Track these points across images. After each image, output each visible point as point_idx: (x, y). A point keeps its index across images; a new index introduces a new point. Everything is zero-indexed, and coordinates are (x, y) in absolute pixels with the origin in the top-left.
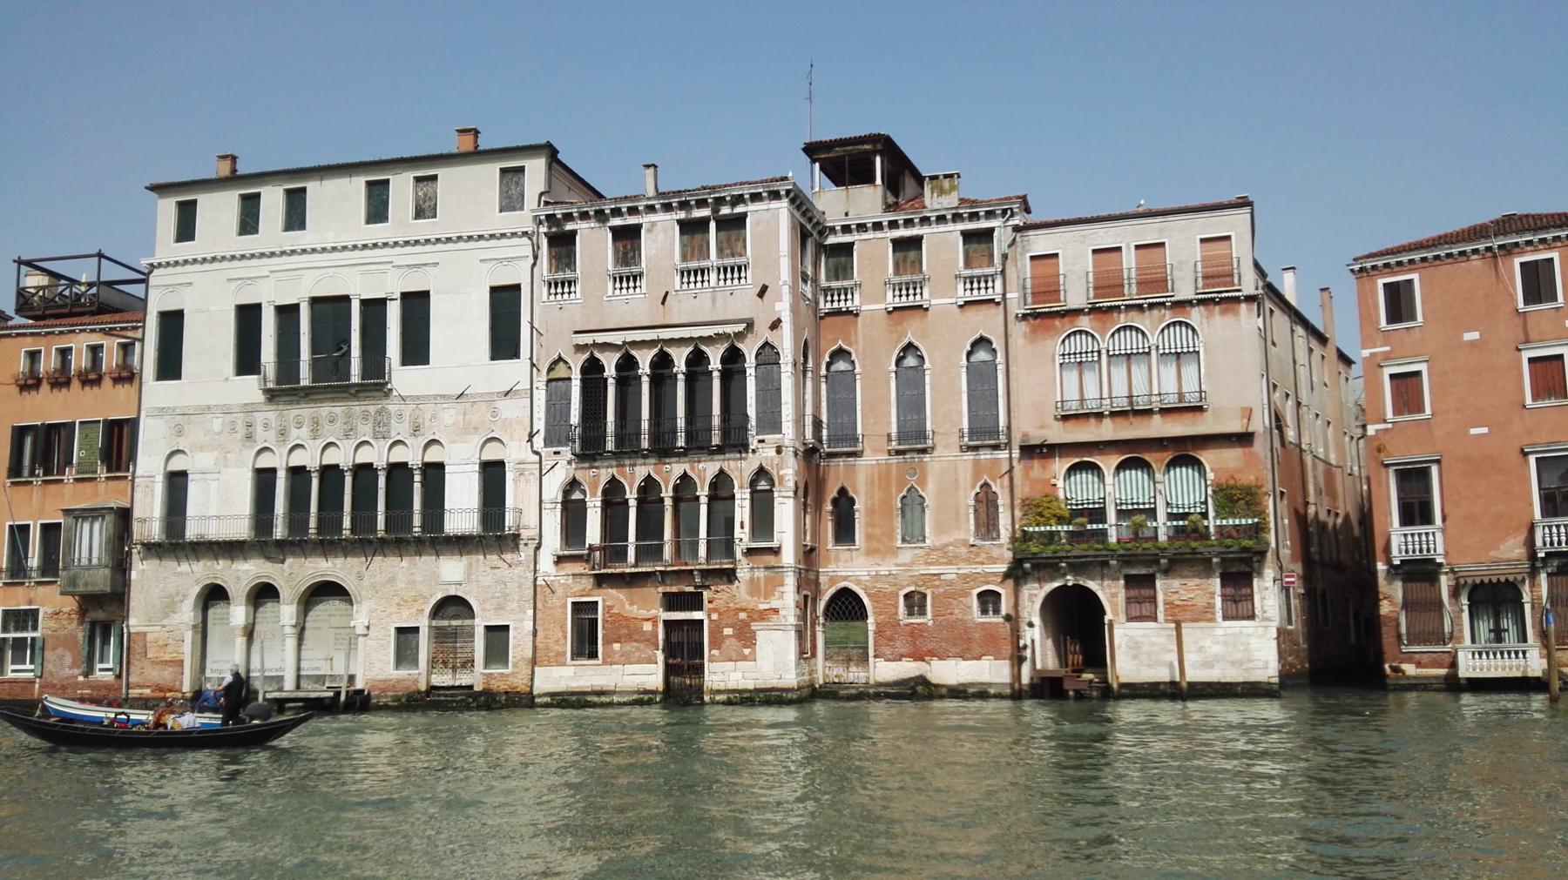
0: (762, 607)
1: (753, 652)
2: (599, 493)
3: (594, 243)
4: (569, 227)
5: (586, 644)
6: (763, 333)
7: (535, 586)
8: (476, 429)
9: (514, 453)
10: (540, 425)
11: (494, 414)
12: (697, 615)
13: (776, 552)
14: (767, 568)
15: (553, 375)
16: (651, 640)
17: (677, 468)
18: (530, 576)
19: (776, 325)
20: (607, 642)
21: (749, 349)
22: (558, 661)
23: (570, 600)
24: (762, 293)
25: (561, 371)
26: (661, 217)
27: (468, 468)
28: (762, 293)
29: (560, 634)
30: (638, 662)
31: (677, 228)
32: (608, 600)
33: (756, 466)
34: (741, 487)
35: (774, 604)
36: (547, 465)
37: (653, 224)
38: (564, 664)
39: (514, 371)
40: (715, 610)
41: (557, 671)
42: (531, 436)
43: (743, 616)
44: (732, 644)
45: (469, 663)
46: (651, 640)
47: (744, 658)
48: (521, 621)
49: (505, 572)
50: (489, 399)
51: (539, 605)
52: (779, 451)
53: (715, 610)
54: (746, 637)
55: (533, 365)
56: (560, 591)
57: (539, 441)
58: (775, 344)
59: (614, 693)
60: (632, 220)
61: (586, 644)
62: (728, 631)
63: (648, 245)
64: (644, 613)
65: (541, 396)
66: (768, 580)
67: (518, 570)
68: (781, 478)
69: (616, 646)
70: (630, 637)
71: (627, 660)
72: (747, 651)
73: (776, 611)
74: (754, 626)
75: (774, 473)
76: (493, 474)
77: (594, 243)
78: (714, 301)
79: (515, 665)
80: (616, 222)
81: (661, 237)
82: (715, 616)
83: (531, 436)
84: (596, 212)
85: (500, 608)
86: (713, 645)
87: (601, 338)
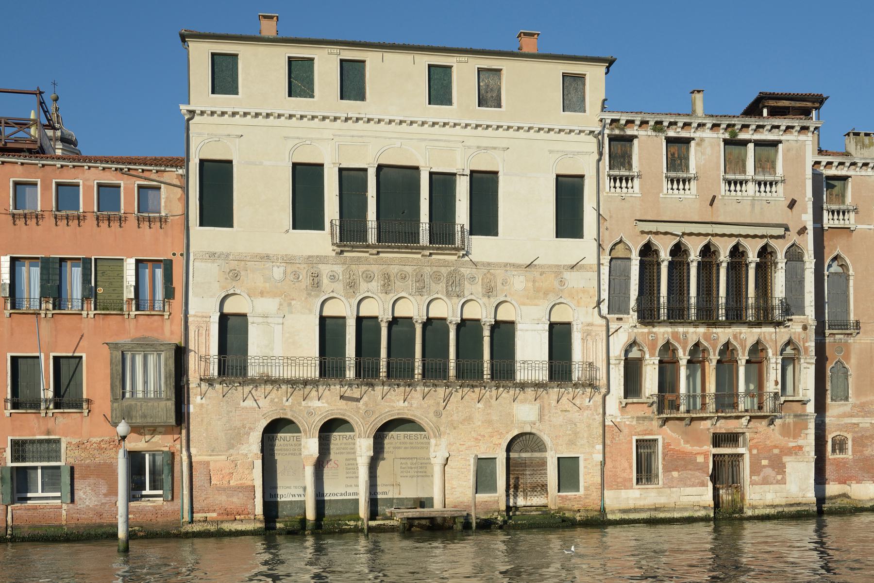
0: (791, 444)
1: (784, 479)
2: (657, 354)
3: (648, 151)
4: (629, 132)
5: (645, 472)
6: (793, 237)
7: (604, 426)
8: (546, 294)
9: (584, 318)
10: (605, 295)
11: (562, 282)
12: (740, 450)
13: (804, 403)
14: (796, 416)
15: (614, 254)
16: (701, 468)
17: (723, 334)
18: (599, 418)
19: (802, 231)
20: (667, 470)
21: (780, 249)
22: (625, 485)
23: (634, 438)
24: (792, 204)
25: (620, 252)
26: (706, 133)
27: (540, 327)
28: (792, 204)
29: (626, 465)
30: (693, 486)
31: (722, 144)
32: (666, 437)
33: (786, 339)
34: (775, 354)
35: (801, 442)
36: (613, 326)
37: (702, 140)
38: (632, 488)
39: (582, 249)
40: (756, 447)
41: (624, 493)
42: (599, 303)
43: (776, 451)
44: (769, 471)
45: (544, 487)
46: (701, 468)
47: (778, 482)
48: (591, 454)
49: (575, 415)
50: (558, 270)
51: (608, 442)
52: (805, 328)
53: (756, 447)
54: (779, 467)
55: (600, 245)
56: (626, 431)
57: (604, 307)
58: (802, 245)
59: (674, 509)
60: (684, 134)
61: (645, 472)
62: (765, 462)
63: (695, 158)
64: (696, 449)
65: (605, 270)
66: (795, 424)
67: (587, 413)
68: (806, 349)
69: (675, 474)
70: (685, 468)
71: (683, 482)
72: (779, 477)
73: (800, 448)
74: (785, 459)
75: (801, 345)
76: (559, 336)
77: (648, 151)
78: (753, 205)
79: (586, 488)
80: (671, 133)
81: (708, 151)
82: (755, 452)
83: (599, 303)
84: (657, 123)
85: (572, 443)
86: (752, 473)
87: (663, 227)
